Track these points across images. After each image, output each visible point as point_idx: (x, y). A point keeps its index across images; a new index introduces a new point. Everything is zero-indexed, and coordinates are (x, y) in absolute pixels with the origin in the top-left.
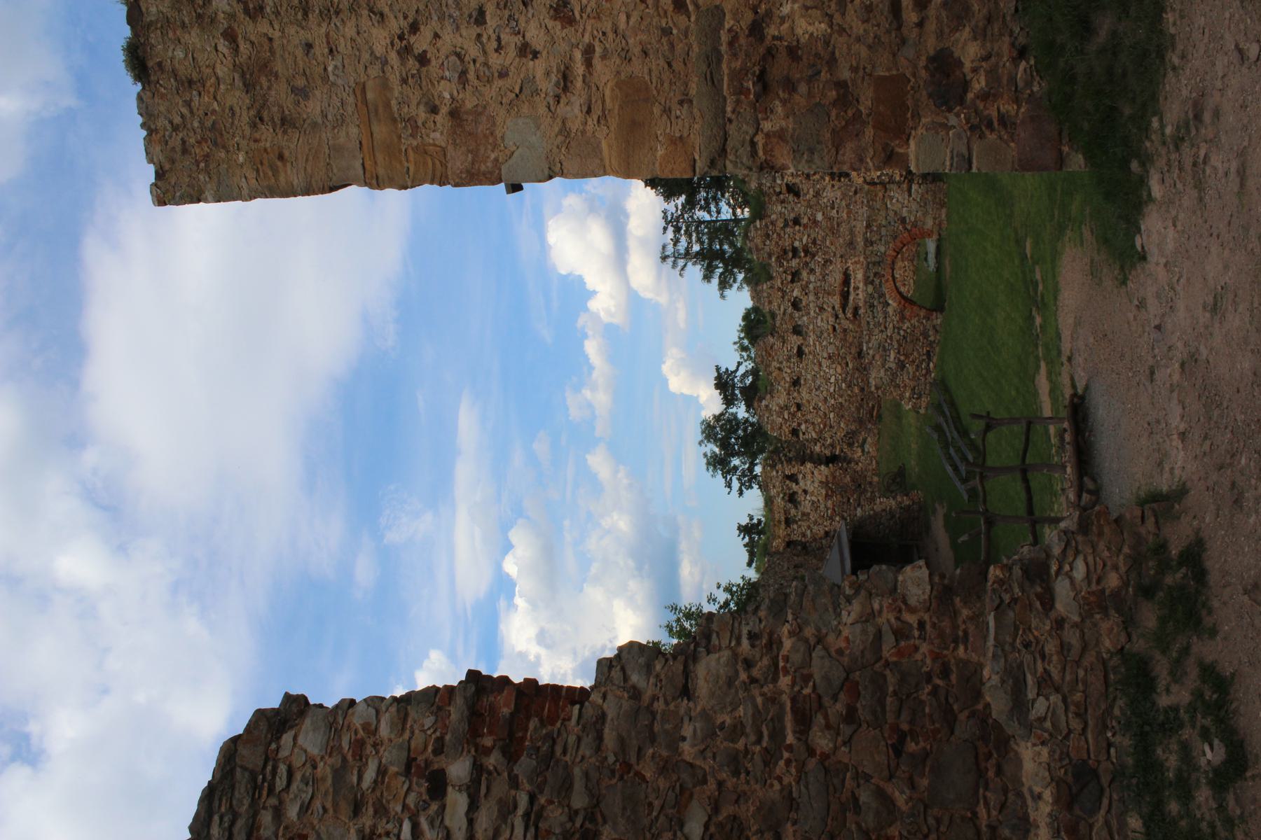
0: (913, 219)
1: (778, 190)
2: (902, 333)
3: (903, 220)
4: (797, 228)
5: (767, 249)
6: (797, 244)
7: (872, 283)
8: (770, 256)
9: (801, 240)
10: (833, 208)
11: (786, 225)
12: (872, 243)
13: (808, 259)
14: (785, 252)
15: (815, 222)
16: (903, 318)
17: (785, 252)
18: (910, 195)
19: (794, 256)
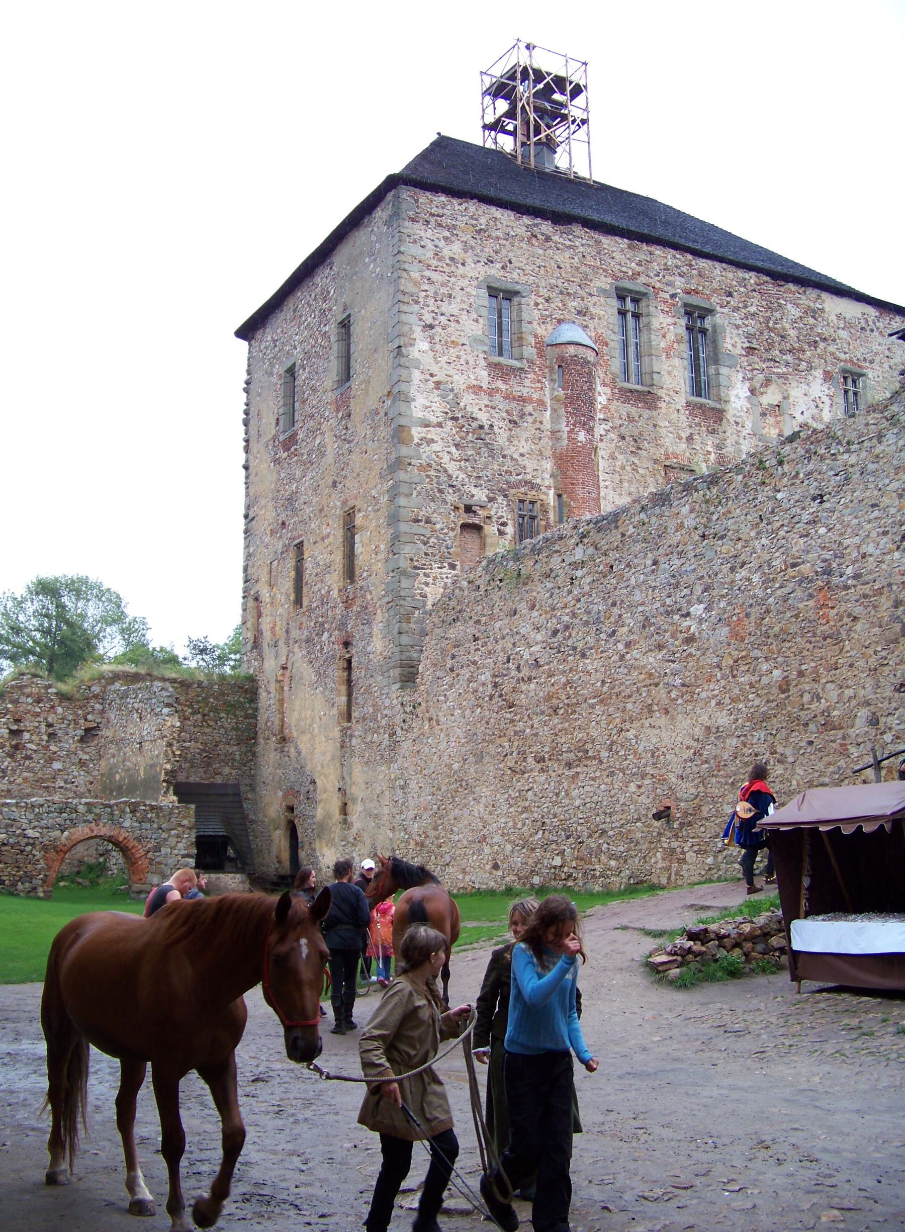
0: (158, 860)
1: (90, 717)
2: (29, 848)
3: (157, 849)
4: (45, 738)
5: (23, 699)
6: (26, 736)
7: (90, 811)
8: (15, 702)
9: (31, 742)
10: (66, 782)
11: (50, 725)
12: (133, 812)
13: (7, 749)
14: (18, 721)
15: (51, 760)
16: (45, 848)
17: (18, 721)
18: (183, 856)
19: (12, 732)
